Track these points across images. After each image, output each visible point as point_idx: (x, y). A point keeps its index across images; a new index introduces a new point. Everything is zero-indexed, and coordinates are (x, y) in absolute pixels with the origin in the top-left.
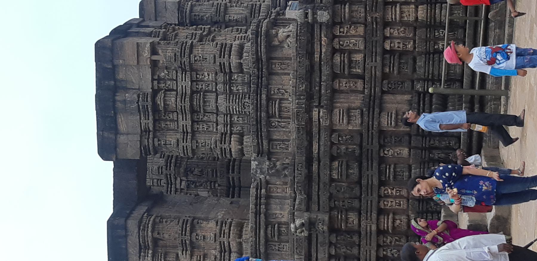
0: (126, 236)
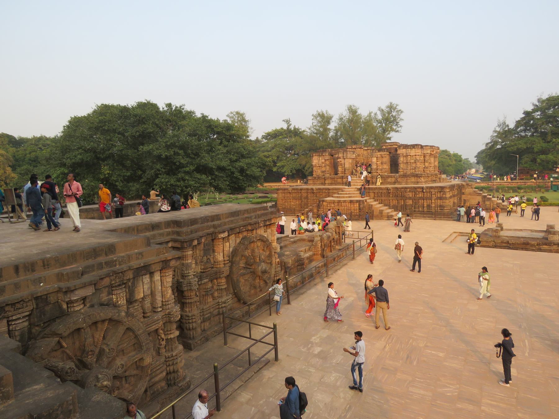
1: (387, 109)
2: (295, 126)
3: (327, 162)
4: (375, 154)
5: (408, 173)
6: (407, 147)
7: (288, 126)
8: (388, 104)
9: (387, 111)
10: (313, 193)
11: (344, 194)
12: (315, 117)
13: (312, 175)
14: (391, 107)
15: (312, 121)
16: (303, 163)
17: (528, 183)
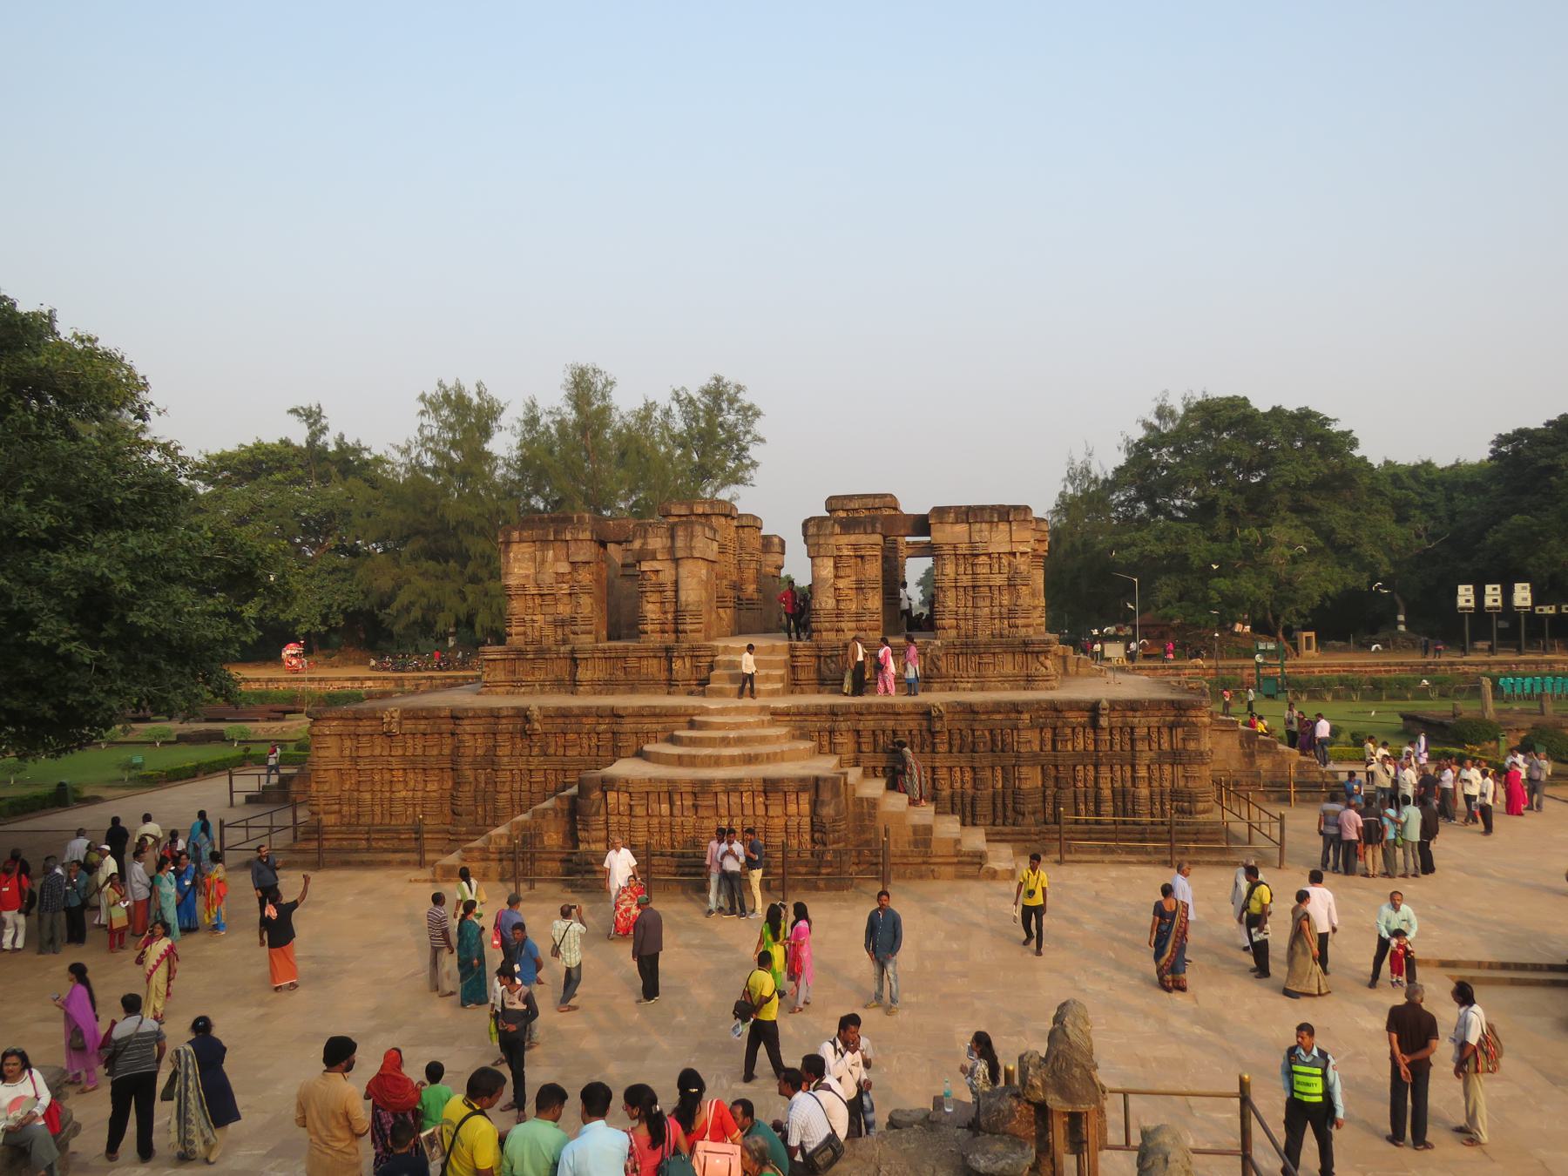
0: (866, 533)
1: (703, 399)
2: (342, 437)
3: (585, 577)
4: (832, 541)
5: (983, 636)
6: (976, 516)
7: (314, 437)
8: (706, 380)
9: (706, 406)
10: (527, 735)
11: (711, 742)
12: (432, 405)
13: (500, 638)
14: (717, 393)
15: (418, 421)
16: (385, 583)
17: (1187, 671)
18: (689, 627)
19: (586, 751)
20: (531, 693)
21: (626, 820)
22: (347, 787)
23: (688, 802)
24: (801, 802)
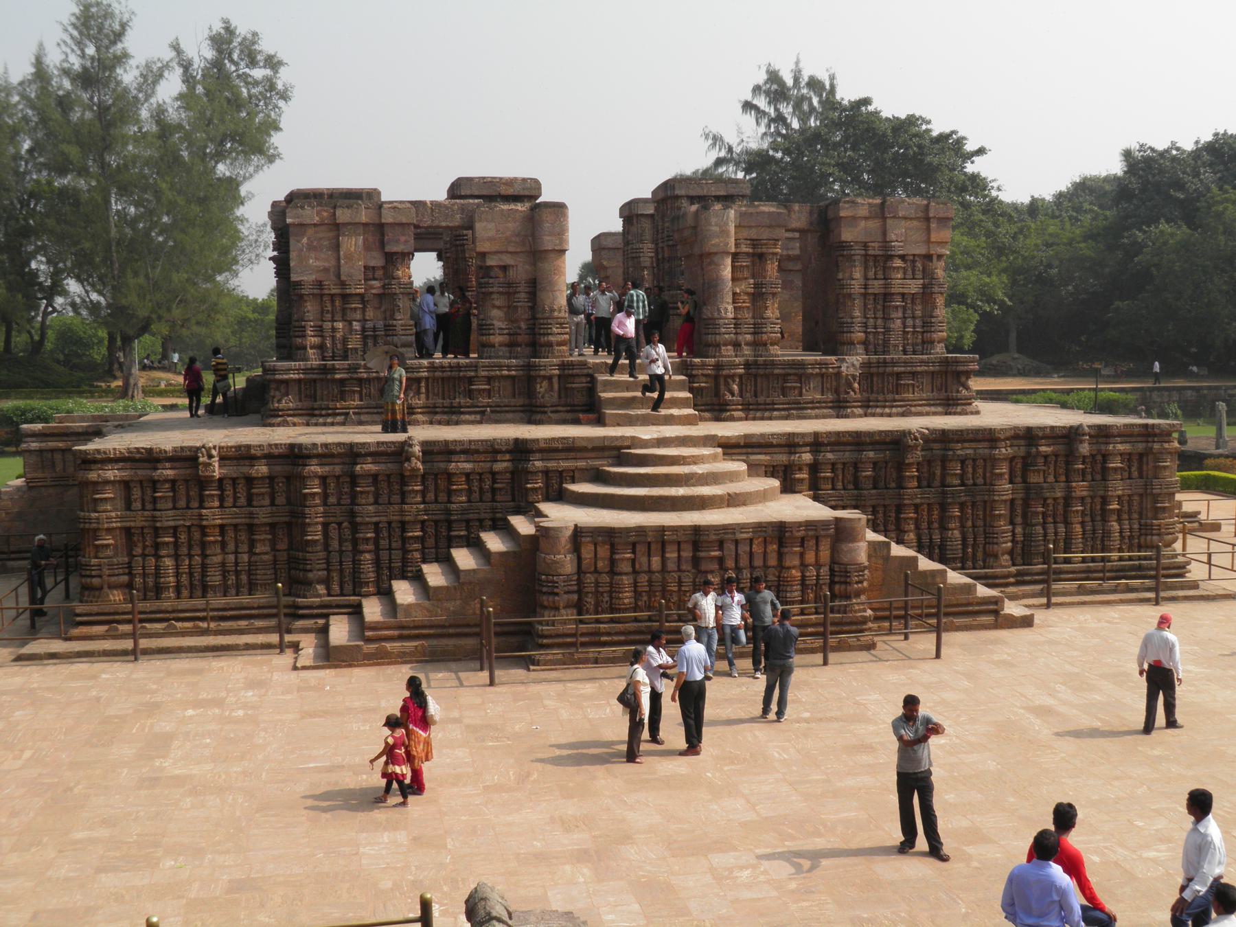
18: (551, 338)
19: (476, 496)
20: (343, 424)
21: (605, 578)
22: (138, 551)
23: (687, 553)
24: (822, 548)
